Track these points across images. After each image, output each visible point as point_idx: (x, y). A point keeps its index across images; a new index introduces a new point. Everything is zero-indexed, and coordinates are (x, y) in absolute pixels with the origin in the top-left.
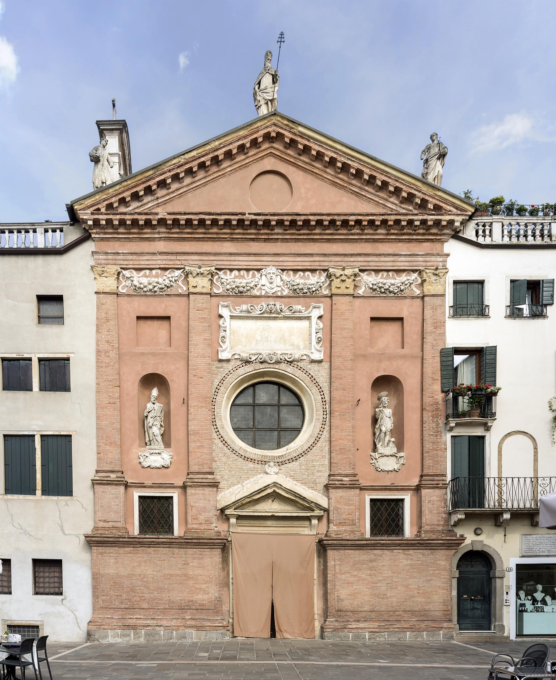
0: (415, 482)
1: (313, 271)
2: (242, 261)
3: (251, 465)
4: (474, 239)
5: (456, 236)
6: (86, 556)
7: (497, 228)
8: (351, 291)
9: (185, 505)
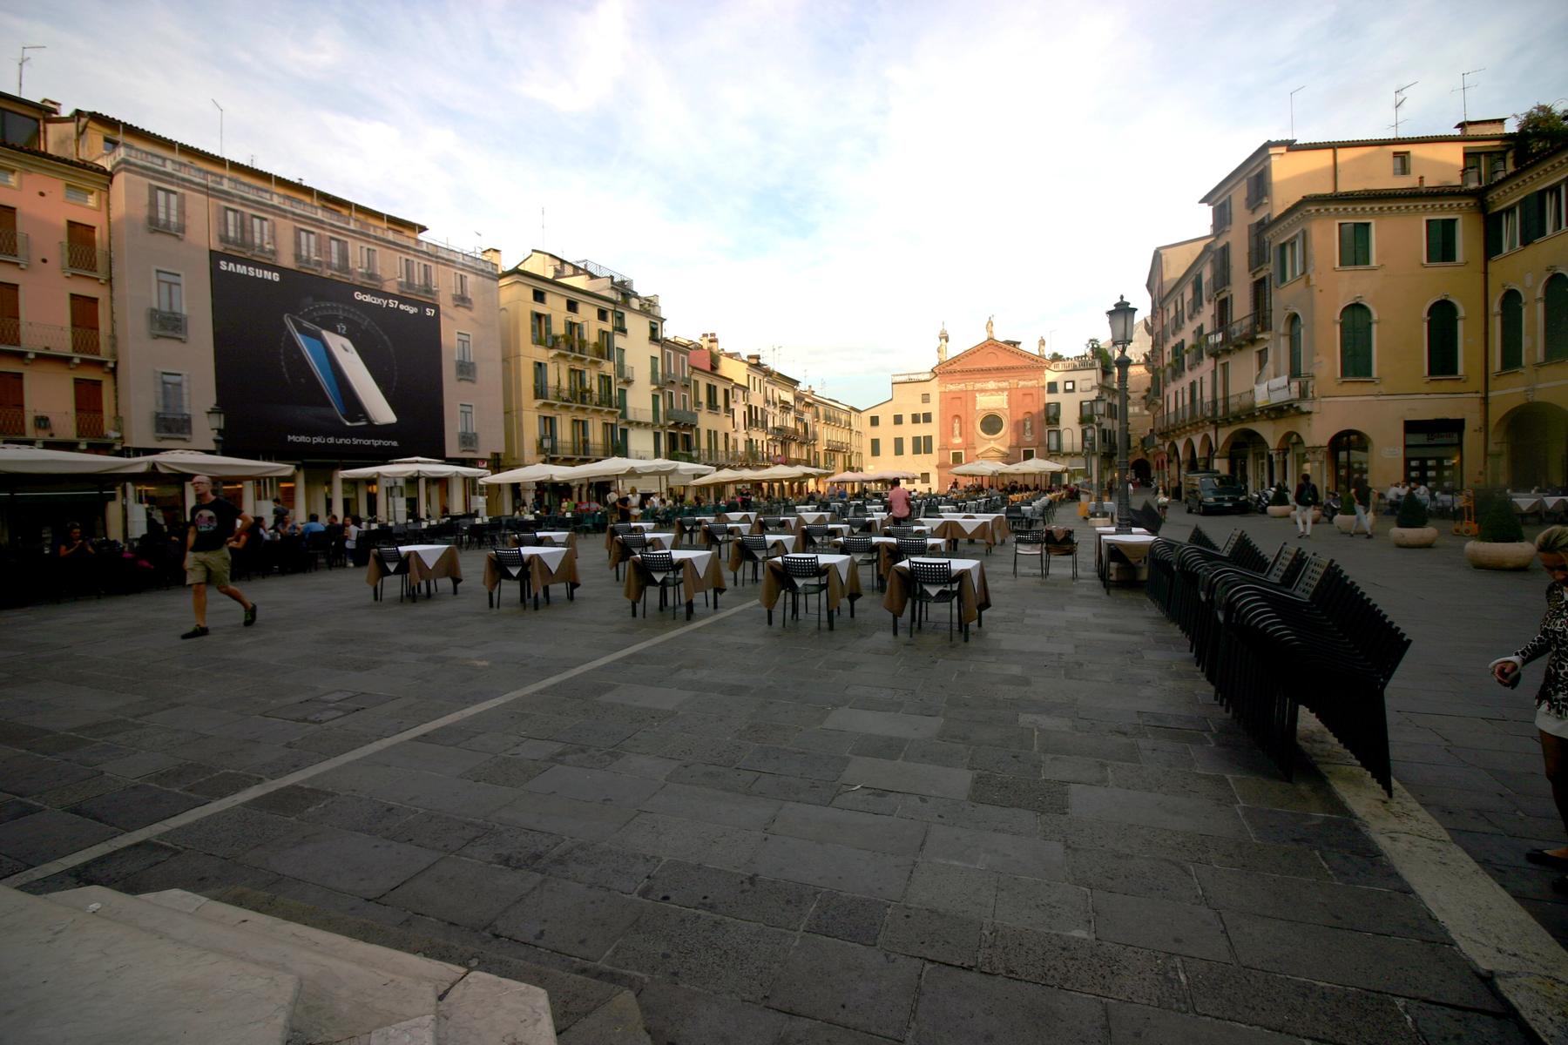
0: (1037, 444)
5: (1048, 368)
6: (937, 470)
9: (966, 454)
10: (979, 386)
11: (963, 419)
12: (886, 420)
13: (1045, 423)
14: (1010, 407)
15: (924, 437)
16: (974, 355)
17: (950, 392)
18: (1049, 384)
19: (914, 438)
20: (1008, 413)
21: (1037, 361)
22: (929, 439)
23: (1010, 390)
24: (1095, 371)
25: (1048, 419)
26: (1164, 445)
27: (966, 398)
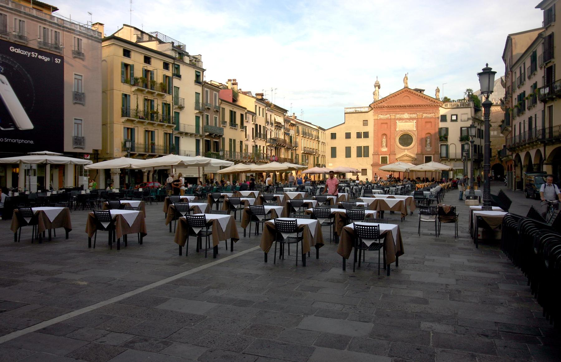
0: (434, 153)
1: (414, 114)
2: (401, 113)
3: (402, 150)
4: (444, 107)
6: (371, 168)
7: (449, 105)
8: (421, 117)
10: (398, 116)
11: (388, 136)
12: (341, 135)
13: (439, 140)
14: (417, 129)
15: (364, 146)
16: (396, 97)
17: (380, 119)
18: (441, 116)
19: (357, 147)
20: (416, 133)
21: (434, 102)
22: (367, 148)
23: (417, 119)
24: (470, 109)
25: (440, 138)
26: (512, 155)
27: (390, 124)
